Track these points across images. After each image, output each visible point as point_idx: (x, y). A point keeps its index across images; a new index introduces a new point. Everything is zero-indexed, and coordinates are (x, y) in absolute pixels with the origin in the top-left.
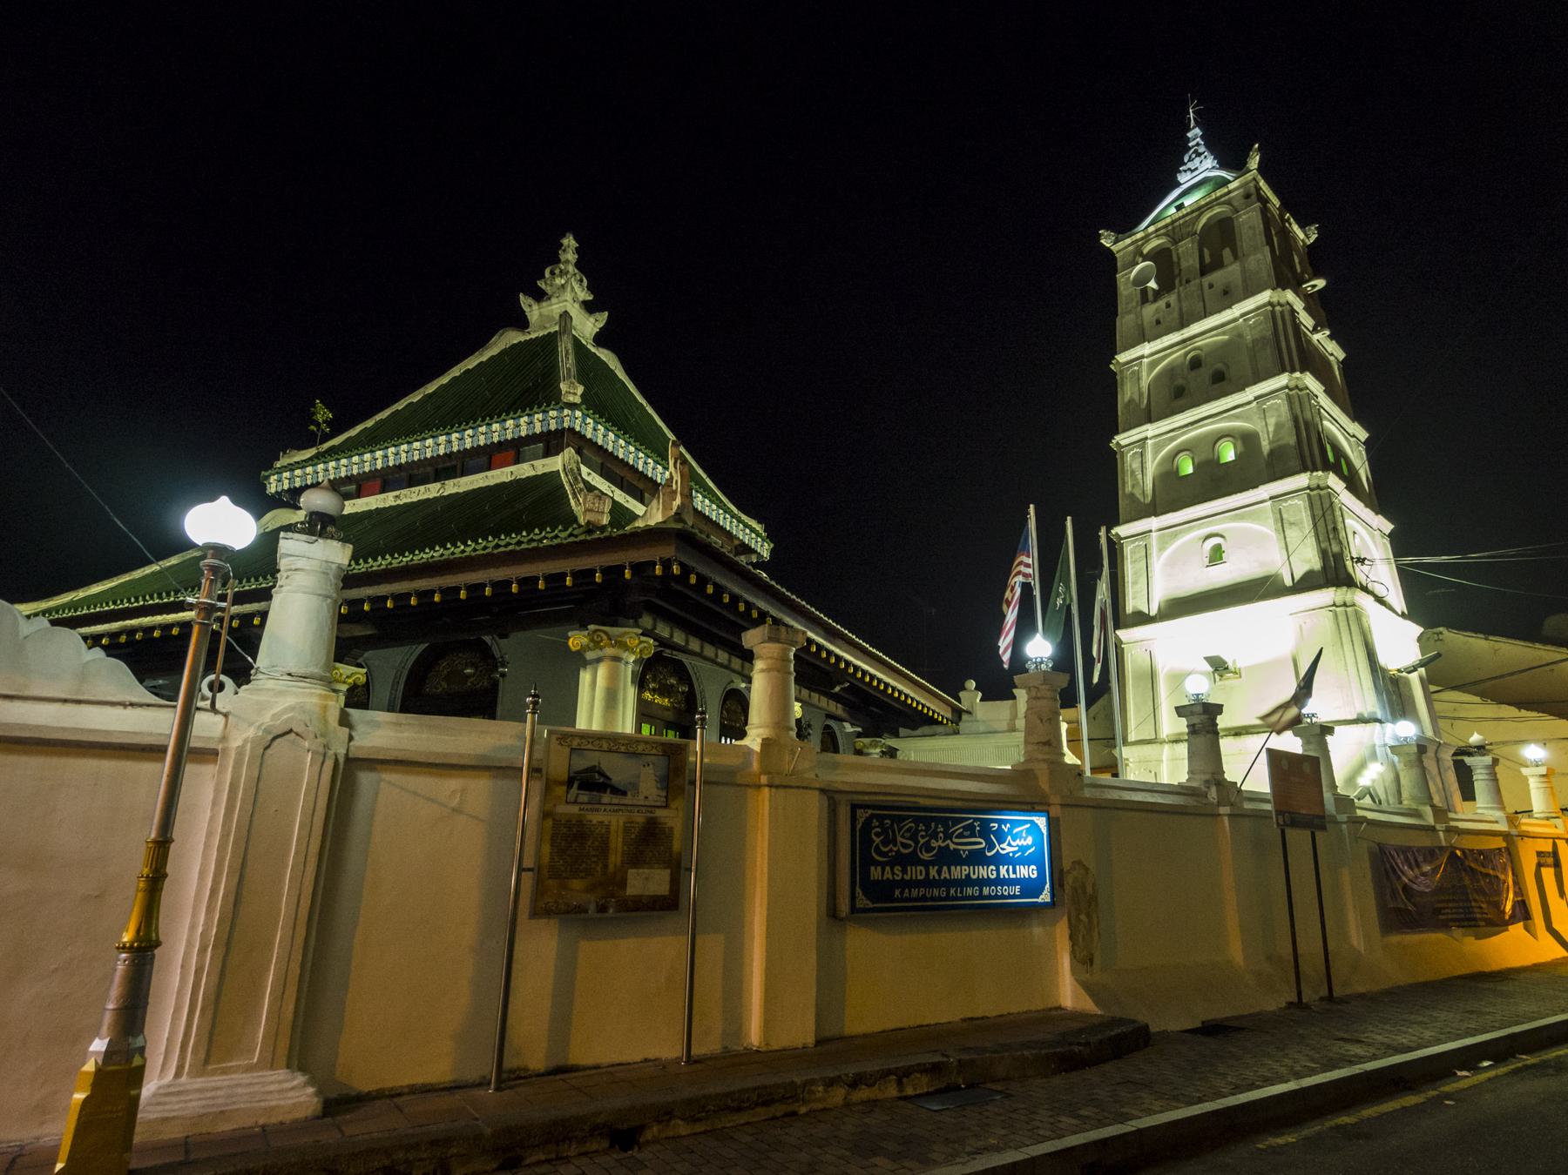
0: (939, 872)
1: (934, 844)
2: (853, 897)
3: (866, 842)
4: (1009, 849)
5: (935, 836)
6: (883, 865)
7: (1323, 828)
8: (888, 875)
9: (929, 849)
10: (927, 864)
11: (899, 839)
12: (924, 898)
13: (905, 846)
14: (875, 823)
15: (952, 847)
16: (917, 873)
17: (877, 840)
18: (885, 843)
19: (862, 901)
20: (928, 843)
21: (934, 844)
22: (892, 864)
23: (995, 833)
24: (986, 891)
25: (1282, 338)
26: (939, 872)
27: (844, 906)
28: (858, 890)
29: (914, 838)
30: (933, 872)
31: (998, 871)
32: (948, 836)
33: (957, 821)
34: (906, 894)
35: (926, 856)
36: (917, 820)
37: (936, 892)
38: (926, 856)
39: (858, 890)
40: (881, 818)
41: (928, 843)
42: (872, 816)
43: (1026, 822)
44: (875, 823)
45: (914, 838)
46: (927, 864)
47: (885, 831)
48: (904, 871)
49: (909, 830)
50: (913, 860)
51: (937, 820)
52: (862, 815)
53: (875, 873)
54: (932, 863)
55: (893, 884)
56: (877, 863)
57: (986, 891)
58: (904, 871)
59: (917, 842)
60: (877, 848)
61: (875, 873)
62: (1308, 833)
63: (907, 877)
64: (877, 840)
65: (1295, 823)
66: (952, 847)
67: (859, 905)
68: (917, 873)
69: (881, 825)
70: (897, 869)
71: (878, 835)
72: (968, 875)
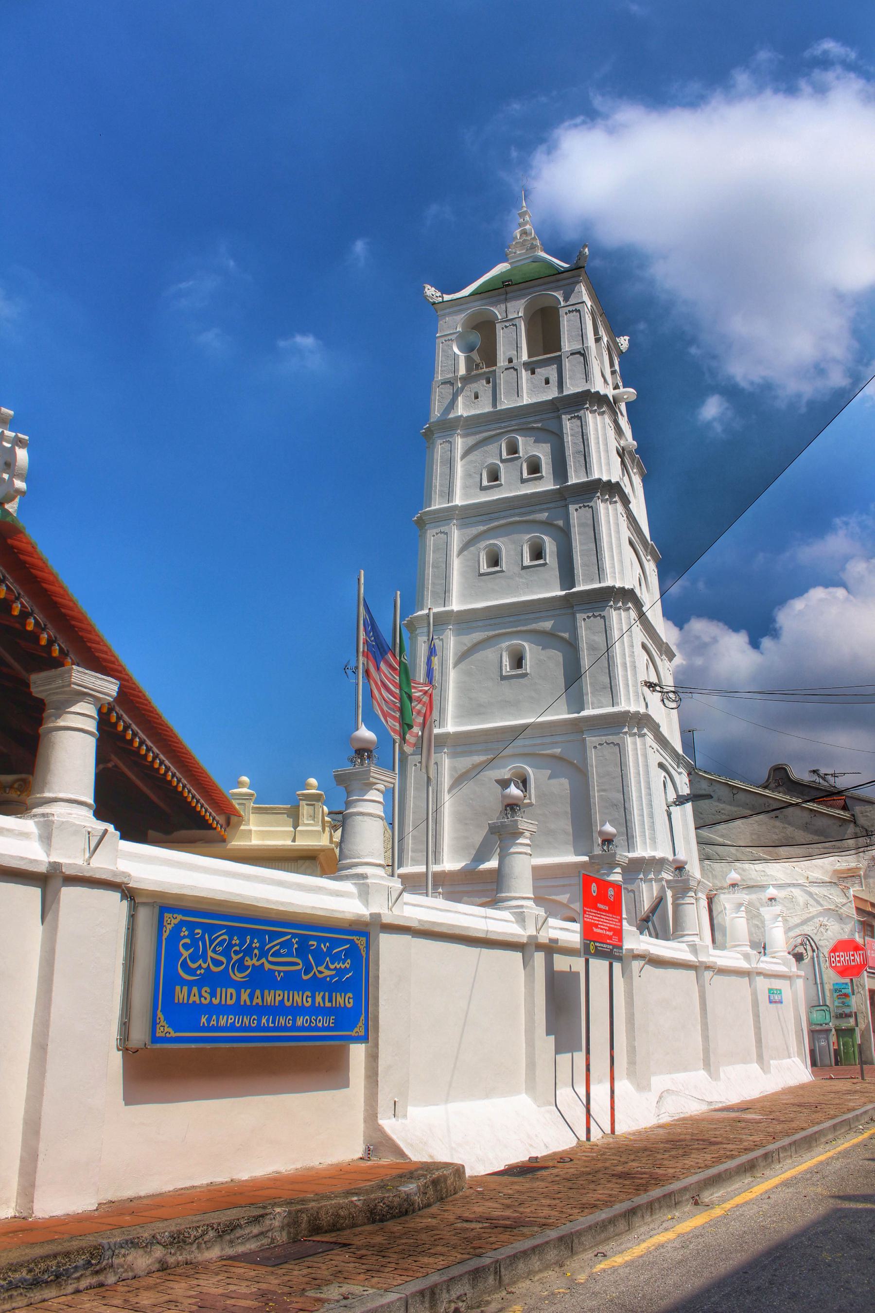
1: (249, 962)
2: (154, 1024)
3: (173, 955)
4: (327, 973)
5: (249, 952)
6: (190, 984)
7: (620, 959)
8: (195, 998)
9: (242, 967)
11: (210, 953)
12: (232, 1028)
13: (217, 963)
14: (185, 932)
15: (267, 966)
17: (185, 954)
18: (194, 958)
19: (164, 1029)
20: (242, 958)
21: (249, 962)
22: (200, 984)
23: (313, 952)
24: (299, 1022)
25: (602, 447)
27: (139, 1035)
28: (160, 1014)
30: (245, 996)
31: (313, 998)
32: (263, 954)
33: (274, 935)
34: (213, 1023)
35: (238, 976)
36: (231, 931)
38: (238, 976)
39: (160, 1014)
40: (191, 926)
41: (241, 961)
42: (182, 923)
43: (347, 941)
44: (185, 932)
45: (226, 953)
46: (239, 986)
47: (194, 942)
48: (213, 994)
49: (220, 944)
51: (254, 933)
52: (172, 921)
53: (181, 994)
55: (199, 1009)
56: (183, 982)
58: (213, 994)
59: (229, 959)
60: (184, 965)
61: (181, 994)
62: (607, 963)
63: (216, 1001)
65: (600, 954)
66: (267, 966)
67: (159, 1034)
68: (227, 996)
69: (192, 935)
70: (206, 990)
71: (186, 946)
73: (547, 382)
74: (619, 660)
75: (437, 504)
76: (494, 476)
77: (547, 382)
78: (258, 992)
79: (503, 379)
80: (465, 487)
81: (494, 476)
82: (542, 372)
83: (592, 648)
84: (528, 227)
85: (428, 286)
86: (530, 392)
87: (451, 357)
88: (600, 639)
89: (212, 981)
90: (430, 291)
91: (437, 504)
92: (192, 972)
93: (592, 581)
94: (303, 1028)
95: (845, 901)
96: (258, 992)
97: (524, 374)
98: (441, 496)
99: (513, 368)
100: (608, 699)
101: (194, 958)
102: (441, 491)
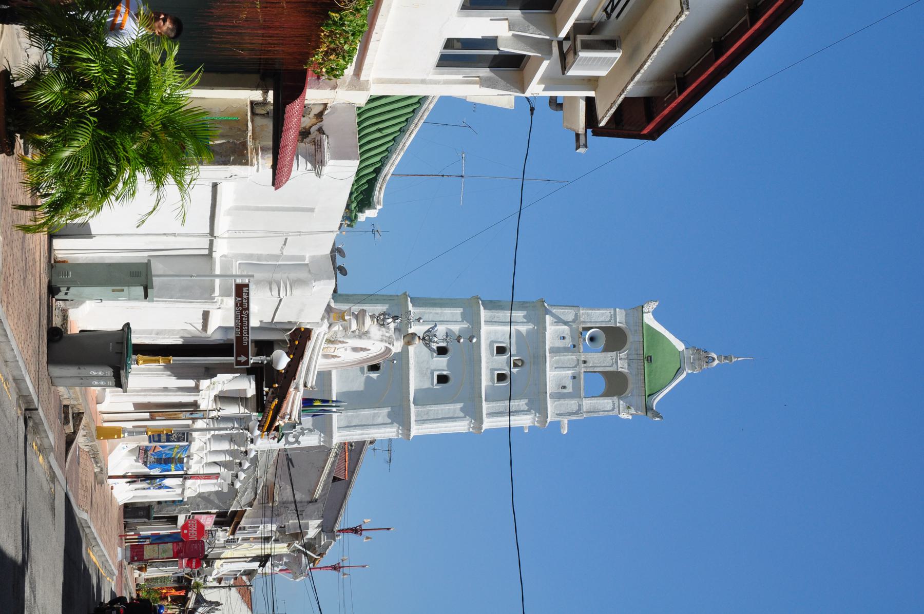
73: (564, 387)
74: (365, 431)
75: (484, 314)
76: (501, 350)
77: (564, 387)
79: (570, 358)
80: (496, 332)
81: (501, 350)
82: (569, 384)
83: (374, 416)
84: (716, 362)
85: (657, 304)
86: (555, 375)
87: (600, 316)
88: (380, 420)
90: (652, 306)
91: (484, 314)
93: (417, 416)
95: (242, 503)
97: (570, 373)
98: (491, 316)
99: (578, 364)
100: (343, 424)
102: (494, 317)
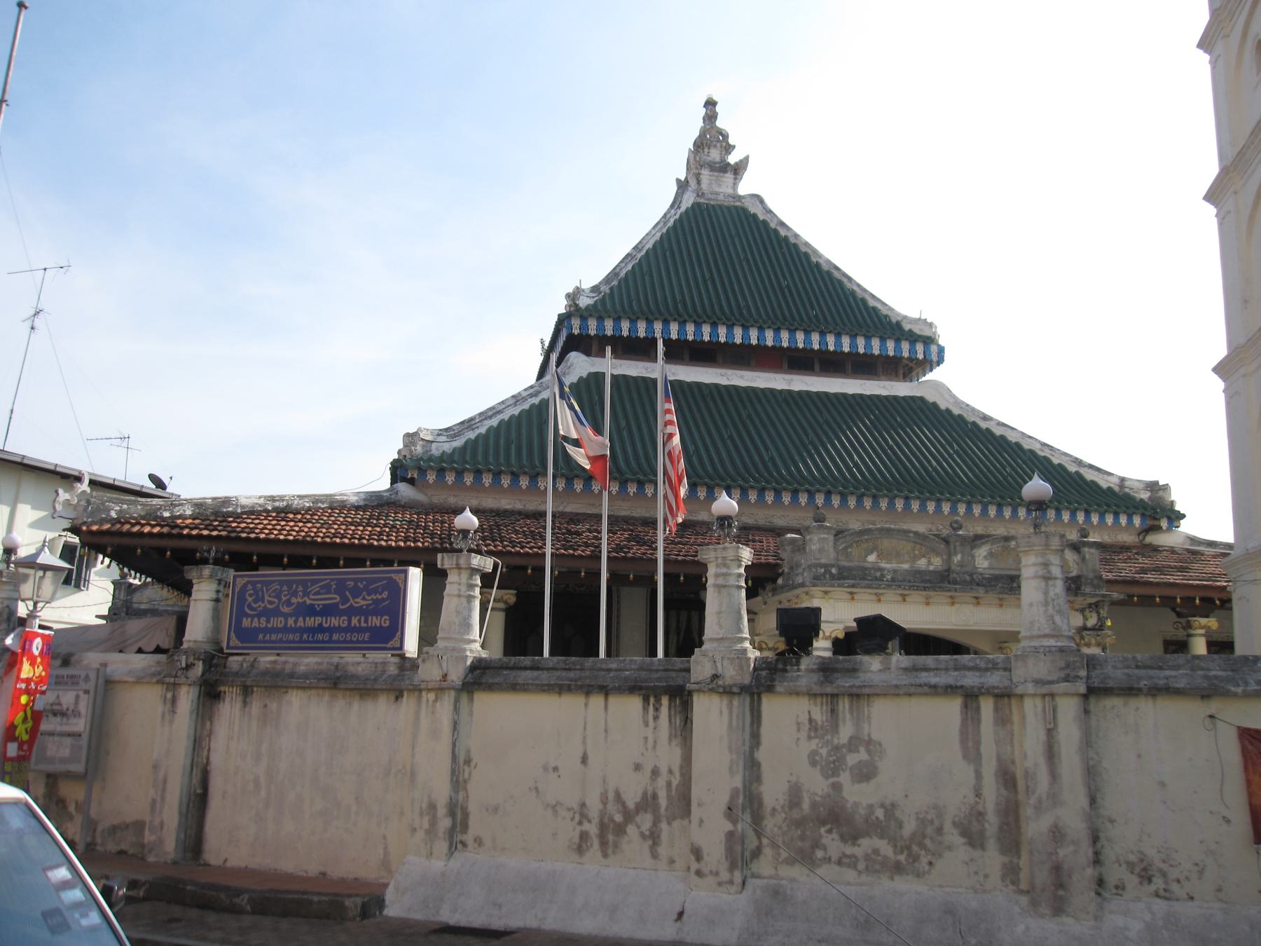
0: (296, 622)
10: (286, 616)
11: (267, 598)
14: (250, 587)
16: (278, 622)
17: (250, 599)
18: (256, 601)
20: (289, 600)
24: (335, 637)
26: (296, 622)
29: (278, 597)
35: (286, 610)
37: (291, 637)
38: (286, 610)
40: (253, 584)
42: (248, 582)
44: (250, 587)
45: (278, 597)
46: (286, 616)
47: (256, 593)
48: (268, 621)
50: (276, 613)
54: (290, 615)
57: (335, 637)
58: (268, 621)
59: (280, 599)
64: (250, 599)
68: (278, 622)
69: (254, 589)
71: (251, 595)
72: (320, 625)
78: (301, 619)
89: (266, 613)
92: (250, 607)
94: (338, 642)
96: (301, 619)
101: (256, 601)
